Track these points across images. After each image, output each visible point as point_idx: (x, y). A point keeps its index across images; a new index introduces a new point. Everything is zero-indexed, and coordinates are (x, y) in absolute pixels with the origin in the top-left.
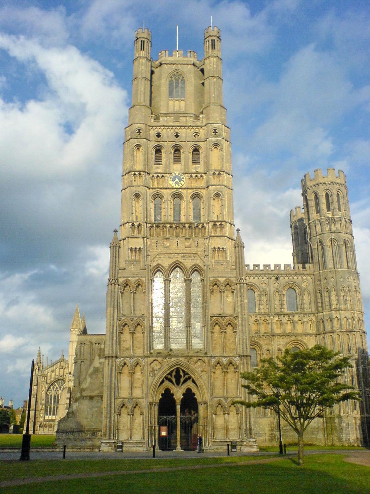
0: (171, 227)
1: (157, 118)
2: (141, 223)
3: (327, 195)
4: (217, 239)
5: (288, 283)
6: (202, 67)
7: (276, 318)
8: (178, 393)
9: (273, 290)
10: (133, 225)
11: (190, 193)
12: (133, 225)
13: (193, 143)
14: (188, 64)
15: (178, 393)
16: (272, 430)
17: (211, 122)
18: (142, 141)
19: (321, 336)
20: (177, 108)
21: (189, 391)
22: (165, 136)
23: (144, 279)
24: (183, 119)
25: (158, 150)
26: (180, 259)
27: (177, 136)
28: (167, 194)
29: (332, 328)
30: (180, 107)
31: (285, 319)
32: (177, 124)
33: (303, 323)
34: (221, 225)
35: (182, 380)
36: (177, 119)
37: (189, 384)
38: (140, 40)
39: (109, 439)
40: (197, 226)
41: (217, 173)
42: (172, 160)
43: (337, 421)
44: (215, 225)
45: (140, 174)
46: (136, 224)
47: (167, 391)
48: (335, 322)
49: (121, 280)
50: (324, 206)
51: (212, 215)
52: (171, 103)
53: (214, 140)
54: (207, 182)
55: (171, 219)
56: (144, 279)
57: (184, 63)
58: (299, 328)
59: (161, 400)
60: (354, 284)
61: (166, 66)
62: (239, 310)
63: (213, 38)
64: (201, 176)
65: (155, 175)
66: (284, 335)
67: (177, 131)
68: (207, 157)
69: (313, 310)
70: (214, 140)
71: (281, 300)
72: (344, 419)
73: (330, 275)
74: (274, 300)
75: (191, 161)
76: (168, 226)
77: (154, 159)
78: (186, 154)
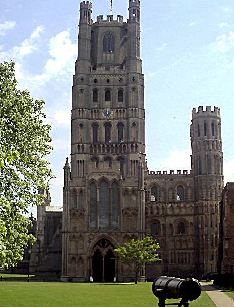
0: (104, 146)
1: (94, 68)
2: (85, 144)
3: (205, 124)
4: (134, 155)
6: (126, 28)
7: (170, 205)
8: (104, 252)
9: (168, 187)
10: (79, 145)
11: (116, 122)
12: (79, 145)
13: (118, 87)
14: (116, 26)
15: (104, 252)
16: (164, 272)
18: (85, 86)
19: (196, 216)
20: (108, 59)
23: (84, 188)
24: (111, 69)
25: (95, 92)
26: (105, 176)
28: (101, 122)
30: (110, 58)
31: (175, 206)
32: (108, 72)
33: (186, 208)
34: (136, 145)
36: (108, 69)
37: (110, 247)
38: (83, 10)
39: (66, 275)
41: (134, 109)
43: (201, 266)
44: (132, 145)
45: (83, 110)
46: (81, 144)
47: (98, 250)
48: (205, 209)
50: (202, 132)
51: (130, 138)
52: (104, 55)
53: (132, 85)
54: (127, 114)
55: (104, 140)
56: (84, 188)
57: (115, 25)
58: (184, 211)
59: (94, 255)
60: (218, 184)
61: (101, 28)
62: (139, 206)
63: (134, 8)
64: (124, 111)
65: (93, 110)
66: (173, 215)
67: (107, 78)
68: (127, 97)
69: (193, 199)
70: (132, 85)
71: (173, 194)
72: (206, 265)
74: (169, 193)
75: (117, 99)
76: (102, 145)
77: (92, 99)
78: (114, 94)
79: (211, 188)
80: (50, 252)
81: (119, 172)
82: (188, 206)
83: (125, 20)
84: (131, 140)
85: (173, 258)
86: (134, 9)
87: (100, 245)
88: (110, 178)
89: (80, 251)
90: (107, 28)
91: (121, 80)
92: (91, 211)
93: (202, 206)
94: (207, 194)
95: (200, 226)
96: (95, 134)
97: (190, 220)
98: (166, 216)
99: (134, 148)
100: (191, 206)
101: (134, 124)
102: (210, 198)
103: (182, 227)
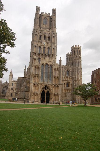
0: (43, 54)
3: (77, 51)
5: (67, 70)
7: (64, 77)
8: (46, 91)
9: (64, 71)
10: (34, 53)
12: (34, 53)
15: (46, 91)
17: (53, 31)
20: (45, 27)
21: (48, 91)
22: (42, 33)
25: (40, 36)
27: (45, 33)
28: (42, 47)
29: (76, 79)
35: (47, 89)
37: (48, 90)
40: (48, 55)
42: (43, 39)
43: (75, 99)
44: (53, 55)
47: (43, 91)
49: (34, 66)
50: (76, 53)
55: (43, 53)
69: (72, 76)
71: (65, 73)
73: (76, 69)
76: (42, 54)
79: (79, 72)
80: (21, 91)
81: (52, 62)
82: (70, 78)
83: (51, 15)
84: (52, 53)
85: (65, 95)
86: (54, 11)
87: (44, 89)
88: (49, 63)
89: (36, 91)
90: (45, 16)
91: (49, 34)
92: (41, 76)
93: (75, 78)
94: (78, 74)
95: (74, 85)
96: (40, 50)
97: (71, 82)
98: (63, 81)
99: (53, 56)
100: (71, 78)
101: (54, 48)
102: (78, 76)
103: (68, 84)
